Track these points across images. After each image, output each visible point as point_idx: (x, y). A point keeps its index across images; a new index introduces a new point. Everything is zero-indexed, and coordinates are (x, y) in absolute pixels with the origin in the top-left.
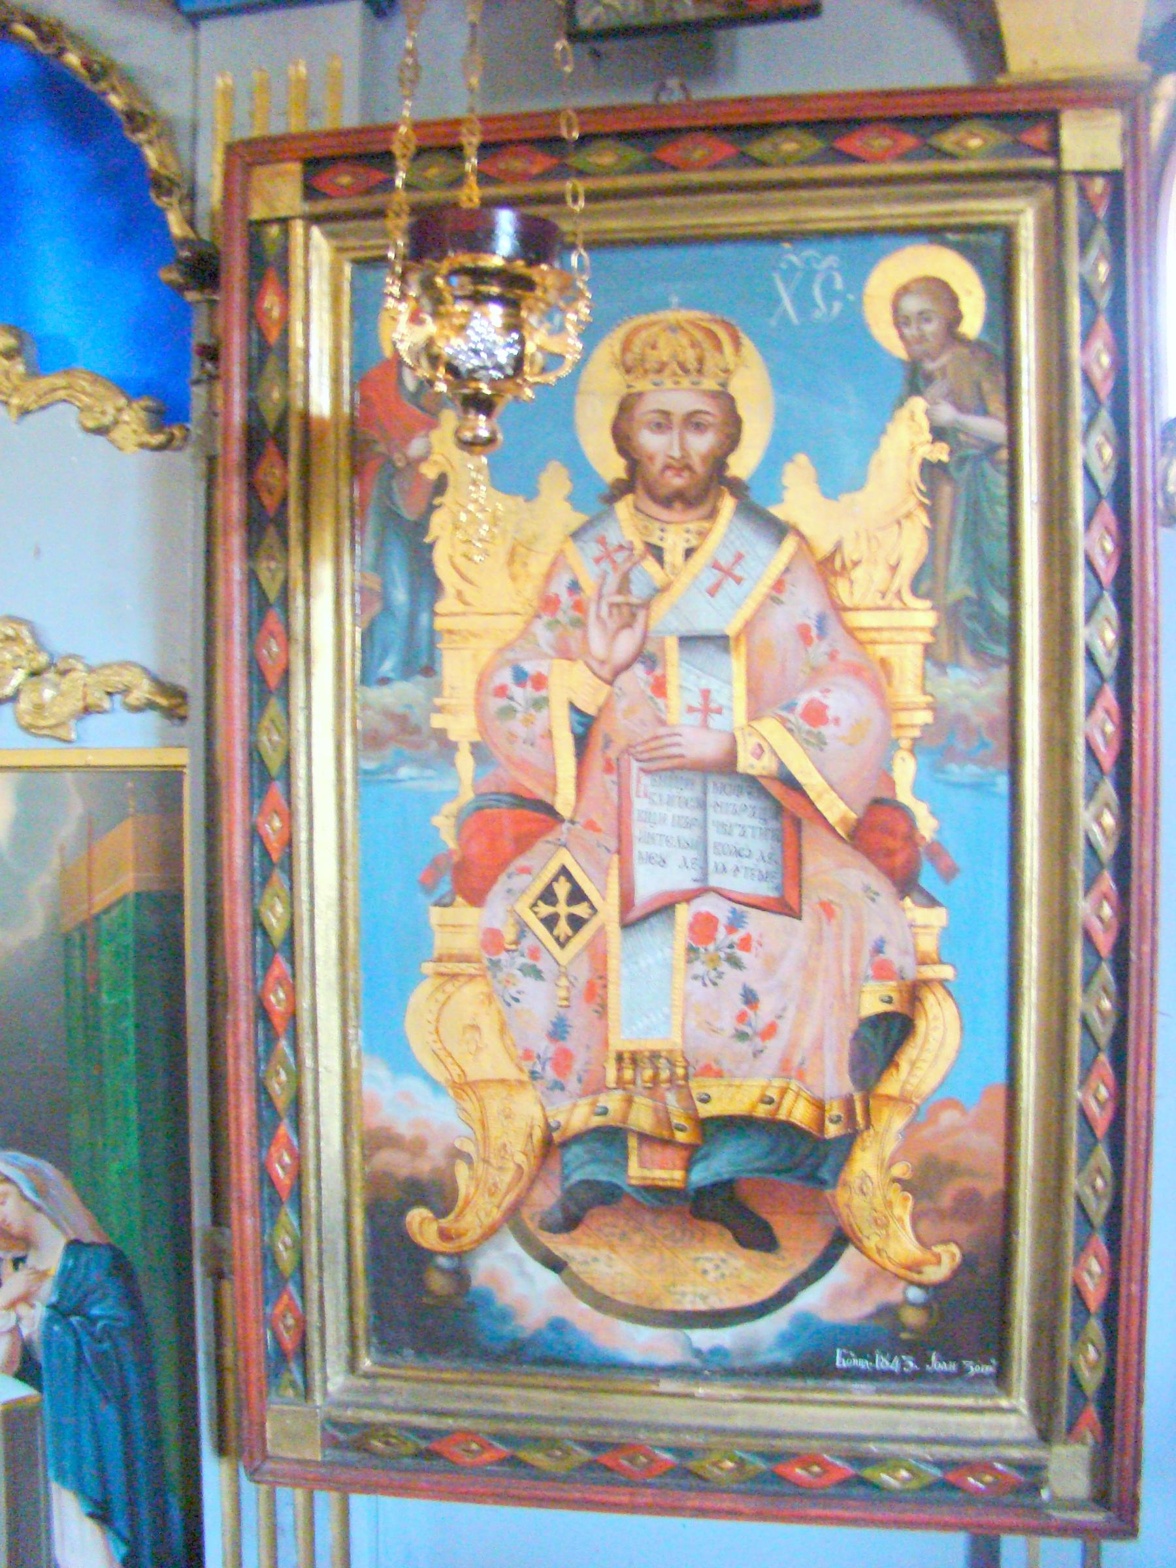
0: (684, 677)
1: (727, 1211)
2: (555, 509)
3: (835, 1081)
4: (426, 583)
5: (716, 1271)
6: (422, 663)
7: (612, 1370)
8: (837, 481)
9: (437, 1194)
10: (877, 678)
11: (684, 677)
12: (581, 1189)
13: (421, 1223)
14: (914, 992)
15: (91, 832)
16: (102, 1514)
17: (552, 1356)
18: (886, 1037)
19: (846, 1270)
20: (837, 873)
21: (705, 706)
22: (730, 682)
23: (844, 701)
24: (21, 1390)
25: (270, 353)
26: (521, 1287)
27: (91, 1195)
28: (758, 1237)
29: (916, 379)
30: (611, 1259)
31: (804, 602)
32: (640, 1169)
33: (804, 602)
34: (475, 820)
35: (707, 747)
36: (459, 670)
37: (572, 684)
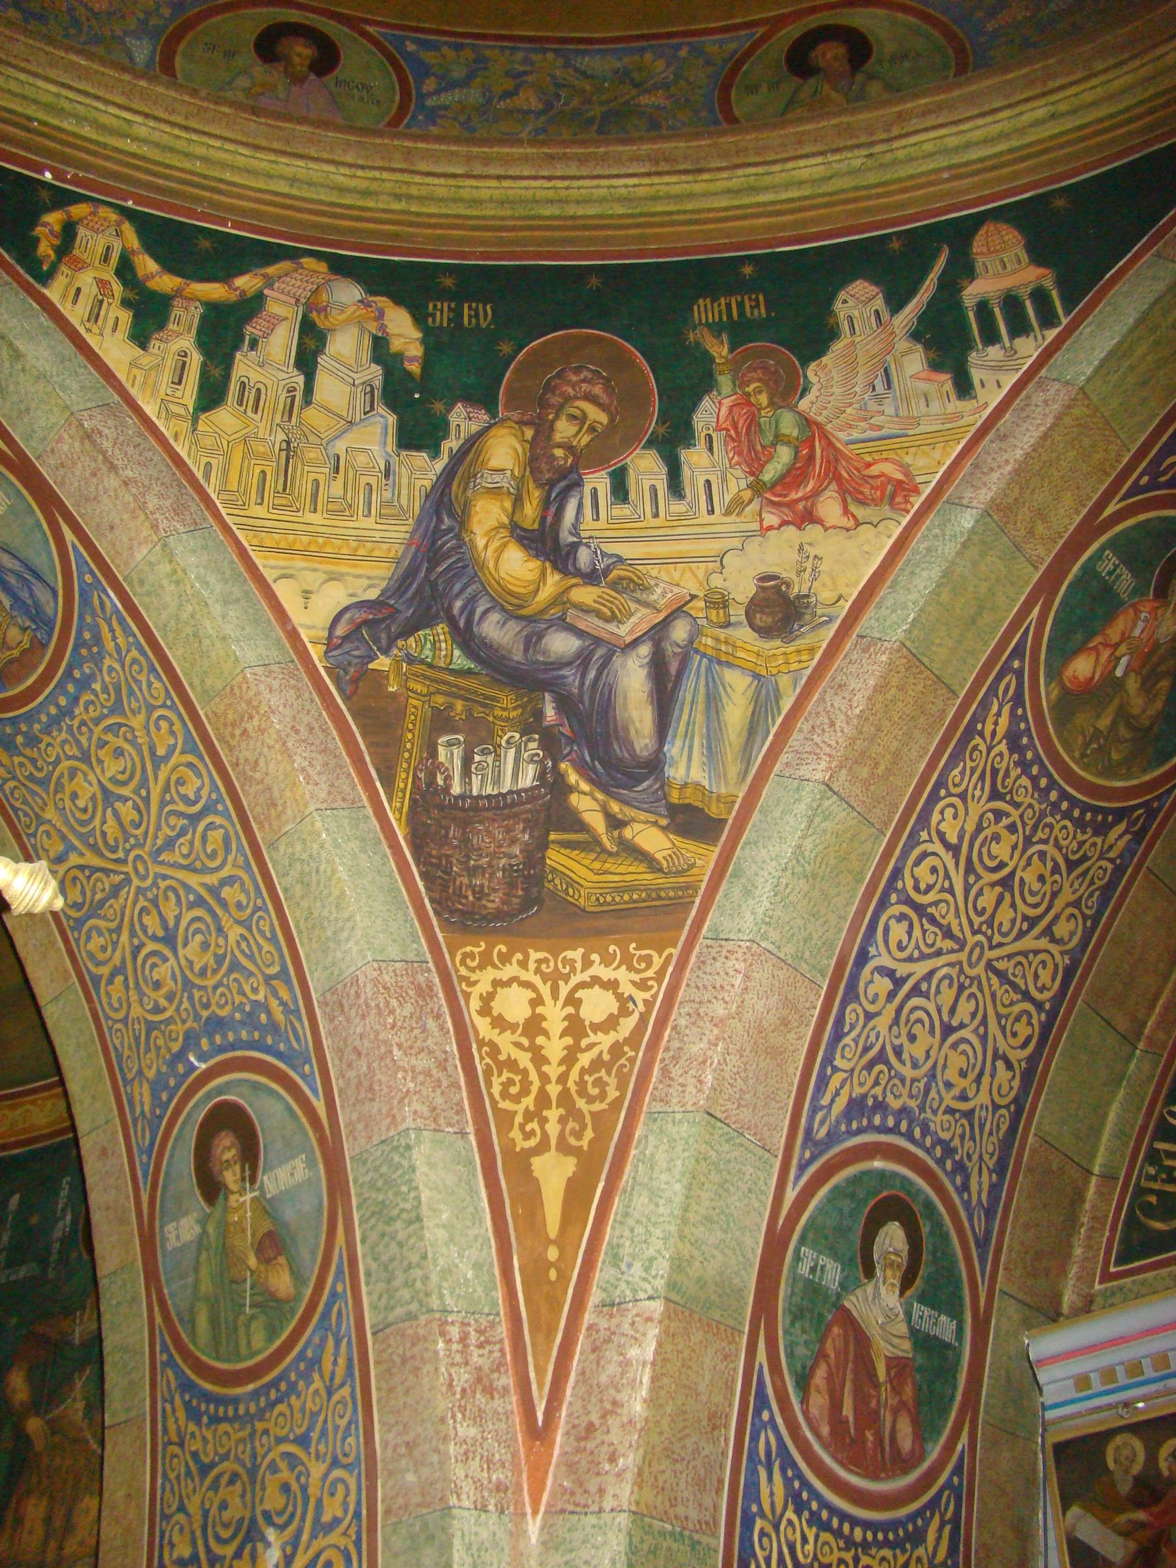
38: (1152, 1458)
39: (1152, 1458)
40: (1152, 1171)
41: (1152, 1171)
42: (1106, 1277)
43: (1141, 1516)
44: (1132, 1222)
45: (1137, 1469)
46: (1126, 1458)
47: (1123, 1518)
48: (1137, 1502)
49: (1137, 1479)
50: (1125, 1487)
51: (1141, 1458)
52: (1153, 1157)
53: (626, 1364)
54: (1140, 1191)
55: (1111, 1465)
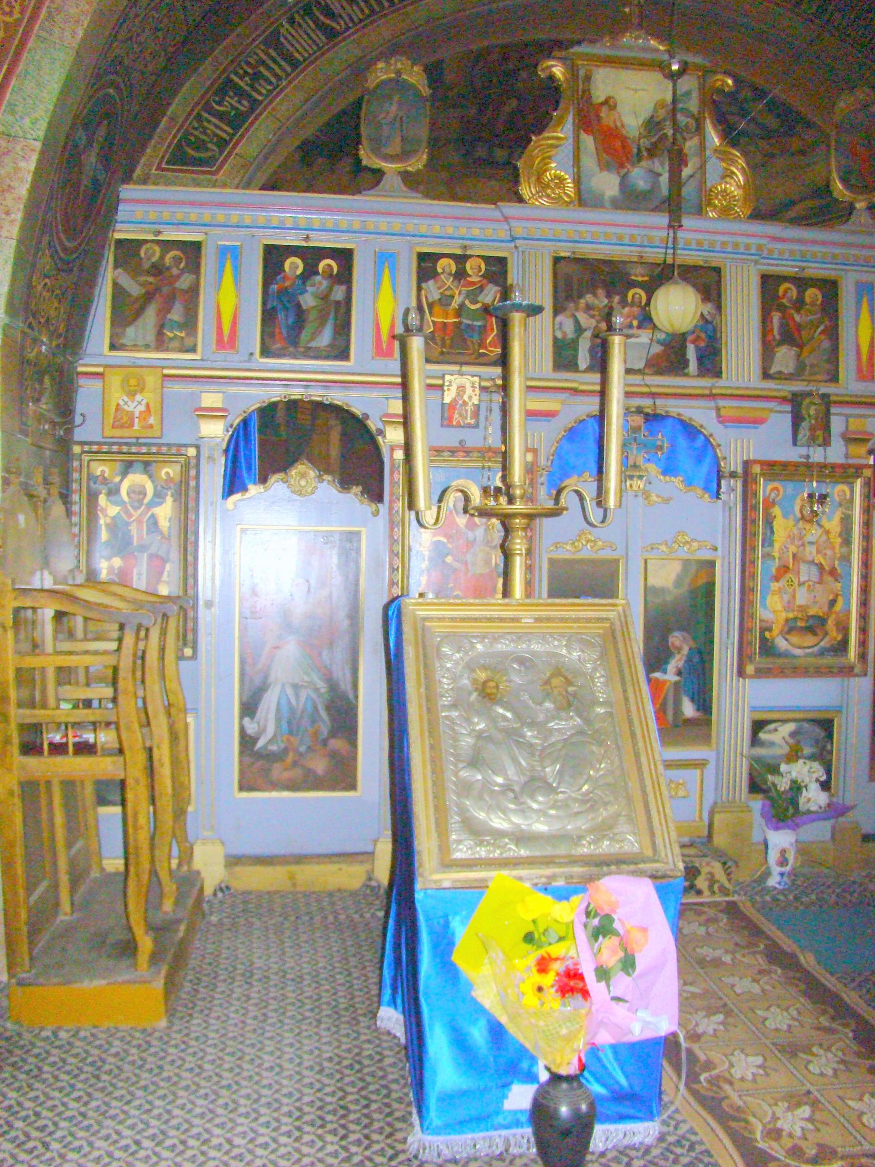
0: (808, 548)
1: (811, 630)
2: (791, 522)
3: (826, 609)
4: (772, 532)
5: (810, 640)
6: (771, 544)
7: (795, 657)
8: (830, 519)
9: (770, 629)
10: (833, 549)
11: (808, 548)
12: (790, 628)
13: (767, 634)
14: (837, 595)
15: (697, 571)
16: (692, 700)
17: (786, 655)
18: (833, 603)
19: (826, 639)
20: (828, 579)
21: (810, 552)
22: (814, 549)
23: (829, 552)
24: (677, 678)
25: (755, 494)
26: (782, 644)
27: (694, 639)
28: (815, 634)
29: (840, 505)
30: (795, 639)
31: (824, 537)
32: (800, 624)
33: (824, 537)
34: (778, 570)
35: (810, 558)
36: (777, 546)
37: (793, 549)
38: (162, 258)
39: (162, 258)
40: (196, 125)
41: (196, 125)
42: (159, 168)
43: (151, 279)
44: (179, 145)
45: (154, 260)
46: (151, 255)
47: (143, 279)
48: (148, 273)
49: (154, 265)
50: (146, 265)
51: (158, 255)
52: (199, 118)
53: (17, 170)
54: (187, 133)
55: (142, 254)
